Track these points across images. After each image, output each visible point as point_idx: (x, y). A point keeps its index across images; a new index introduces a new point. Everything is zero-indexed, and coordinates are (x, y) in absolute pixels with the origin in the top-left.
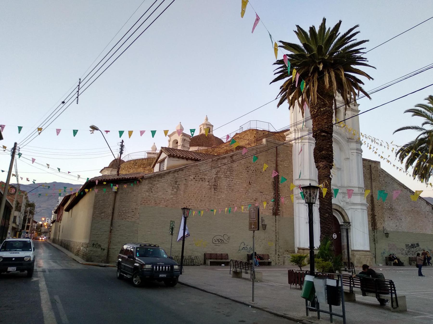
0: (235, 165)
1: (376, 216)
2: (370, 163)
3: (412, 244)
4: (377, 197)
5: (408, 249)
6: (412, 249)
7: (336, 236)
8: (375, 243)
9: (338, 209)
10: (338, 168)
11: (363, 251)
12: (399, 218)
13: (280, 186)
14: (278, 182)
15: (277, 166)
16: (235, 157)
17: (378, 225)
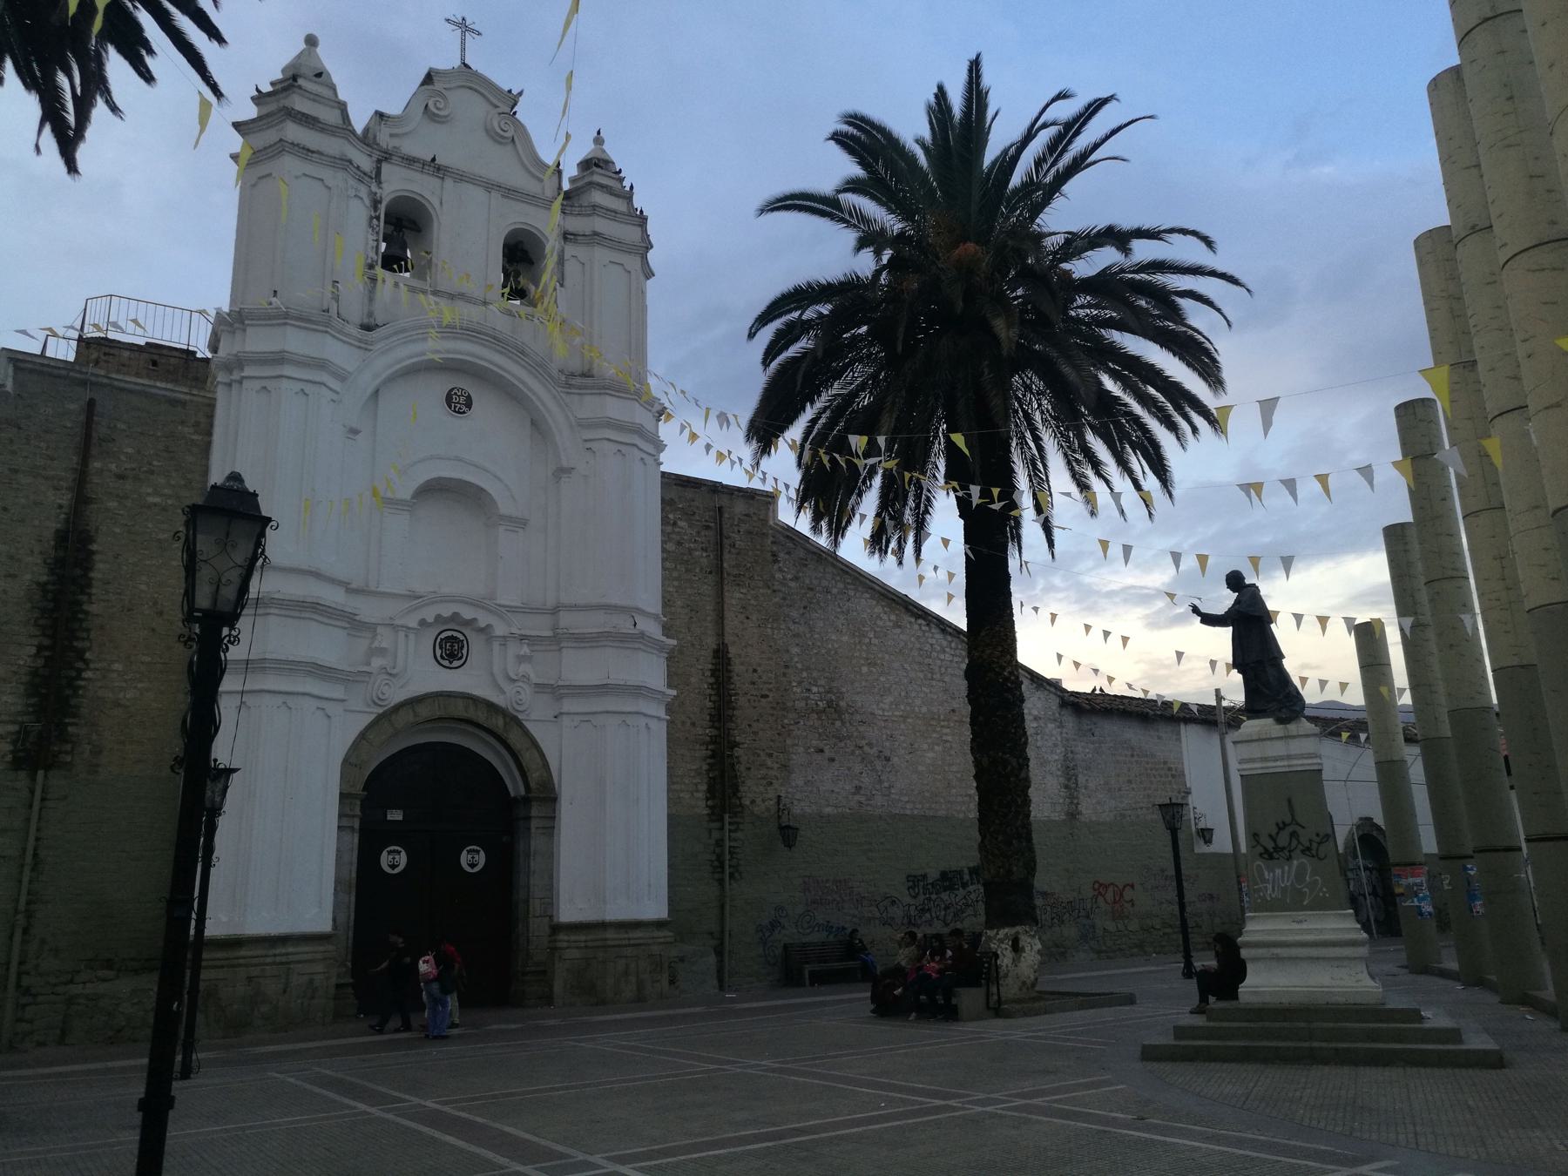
1: (737, 745)
2: (724, 501)
3: (944, 875)
4: (747, 655)
5: (921, 897)
6: (945, 896)
7: (481, 859)
8: (721, 882)
9: (481, 716)
10: (510, 519)
11: (603, 926)
12: (874, 751)
13: (94, 608)
14: (85, 585)
15: (81, 498)
17: (756, 793)
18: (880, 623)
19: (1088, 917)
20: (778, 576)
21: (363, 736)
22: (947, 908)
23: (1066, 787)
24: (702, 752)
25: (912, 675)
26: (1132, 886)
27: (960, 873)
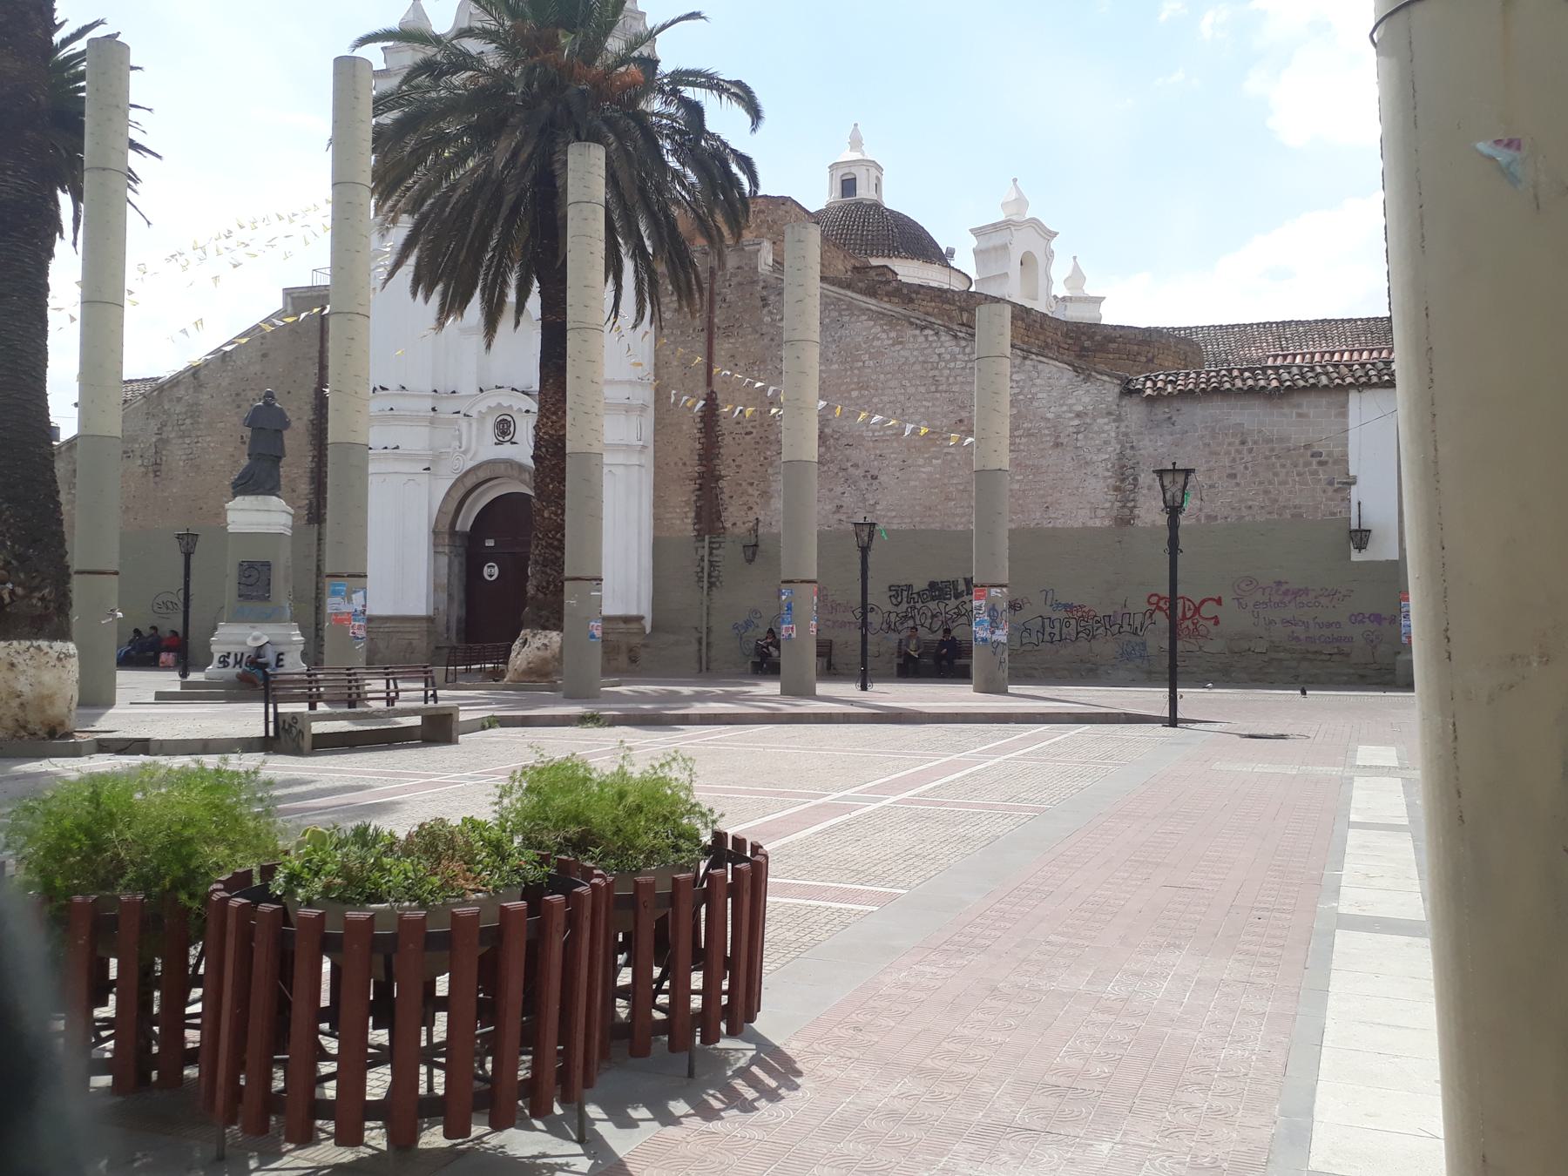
0: (204, 397)
1: (721, 477)
3: (933, 585)
5: (904, 606)
6: (933, 605)
12: (859, 472)
16: (203, 373)
17: (735, 517)
18: (876, 343)
19: (1135, 634)
20: (767, 319)
21: (448, 493)
22: (933, 616)
23: (1117, 489)
24: (694, 487)
25: (911, 390)
26: (1219, 601)
27: (954, 583)
